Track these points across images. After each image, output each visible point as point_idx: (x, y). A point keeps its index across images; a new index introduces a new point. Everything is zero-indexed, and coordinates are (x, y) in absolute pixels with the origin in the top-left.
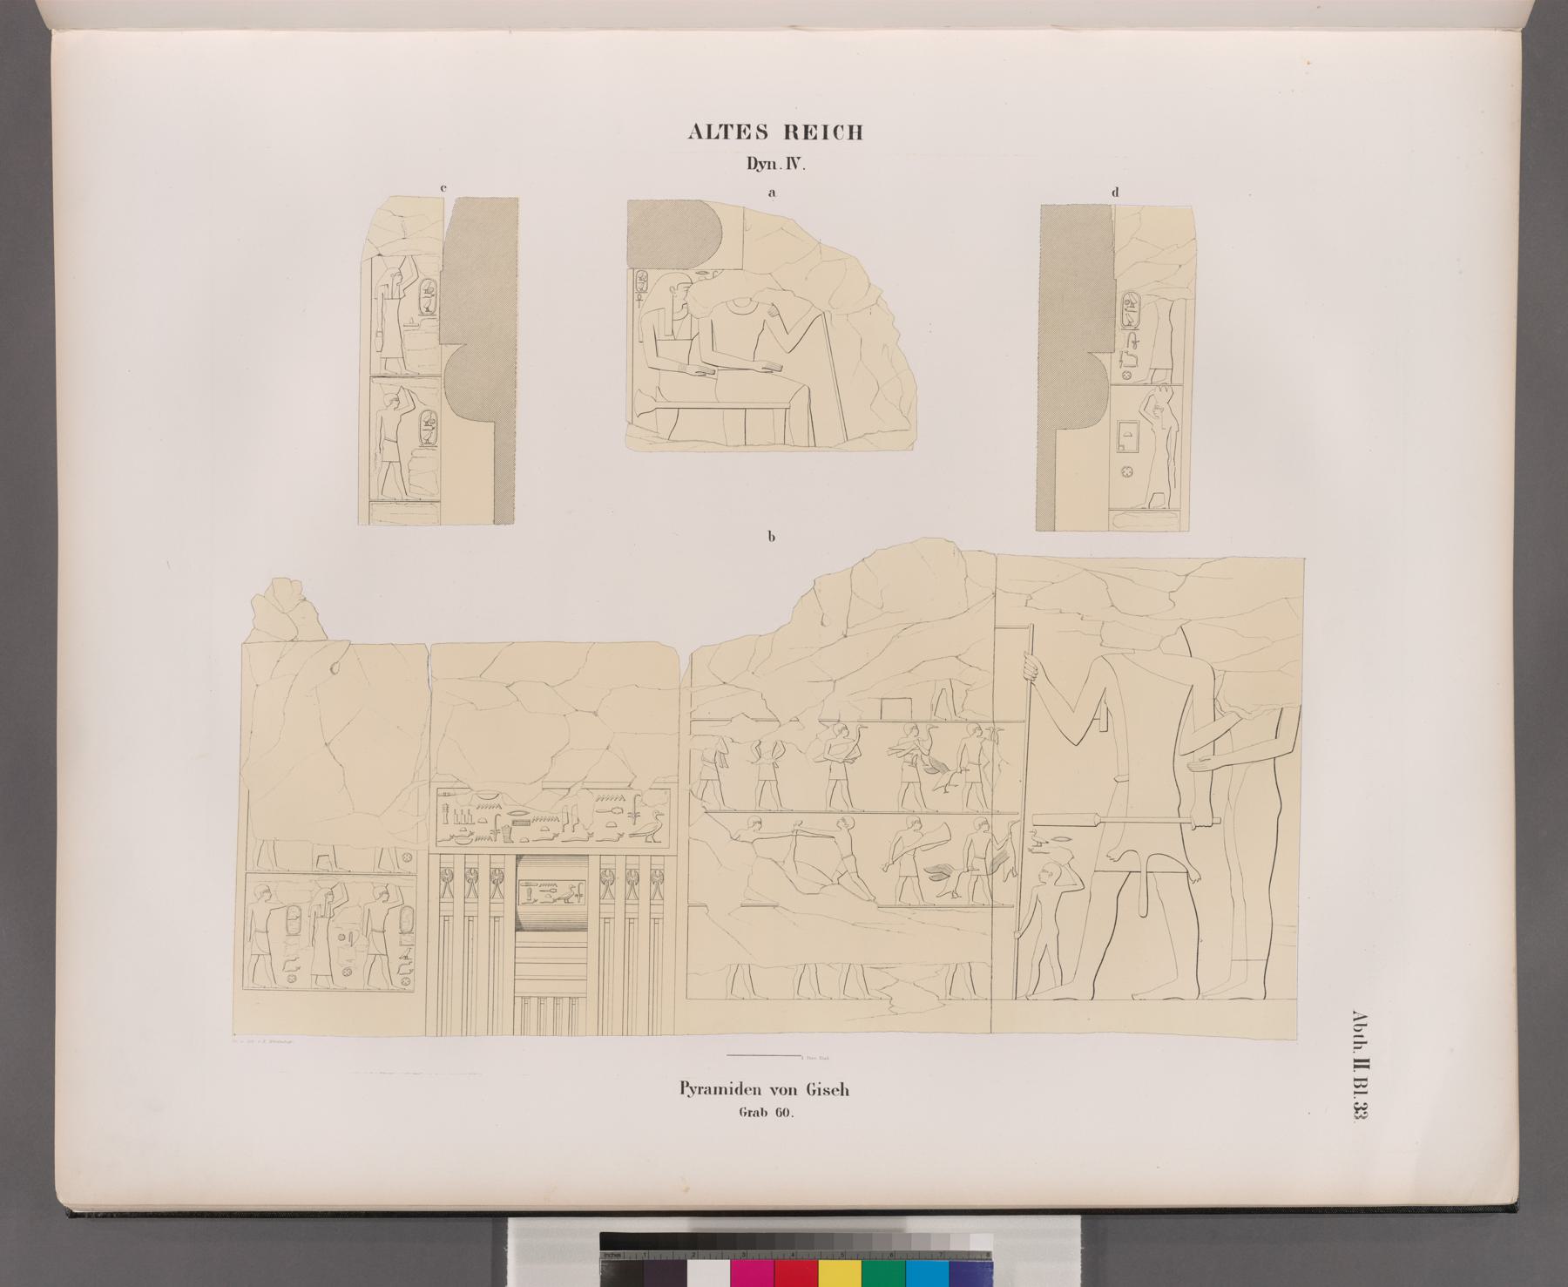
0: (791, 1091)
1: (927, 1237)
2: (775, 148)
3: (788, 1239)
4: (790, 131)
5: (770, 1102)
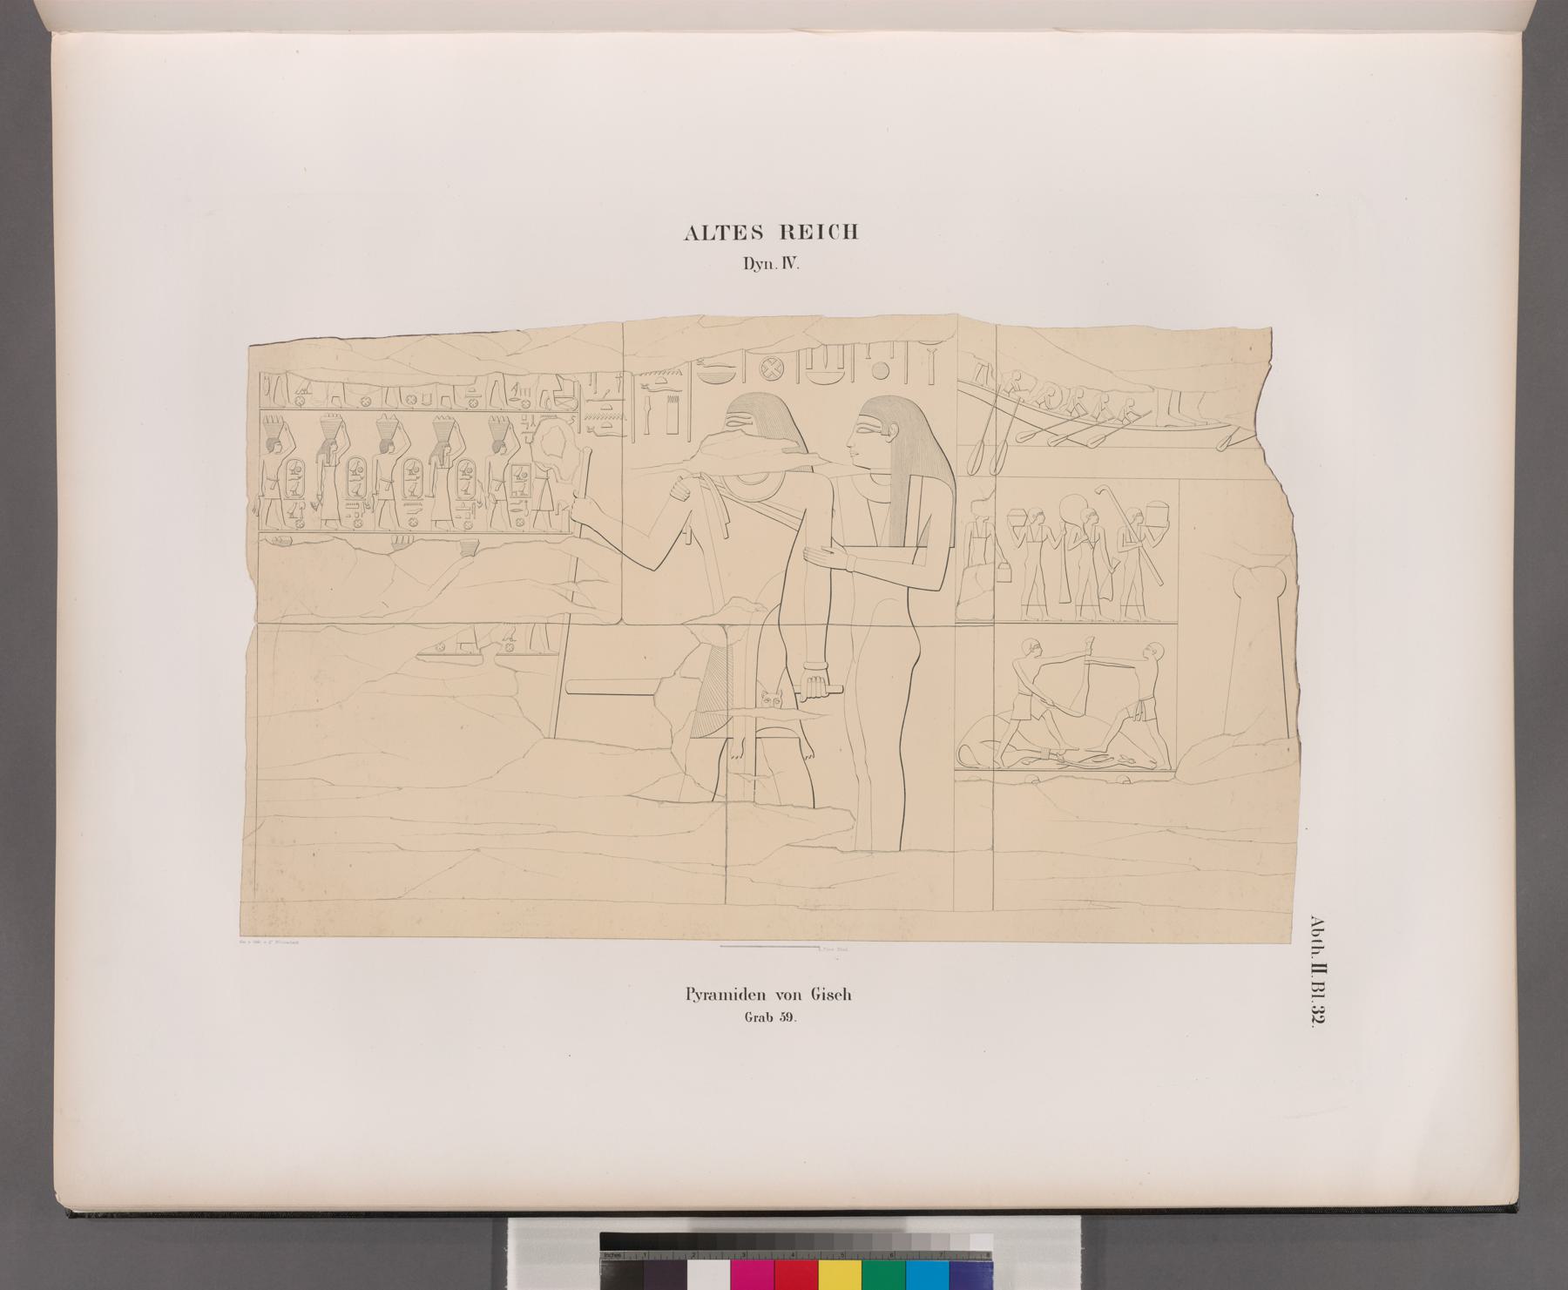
0: (796, 996)
2: (771, 248)
3: (789, 1239)
5: (776, 1007)
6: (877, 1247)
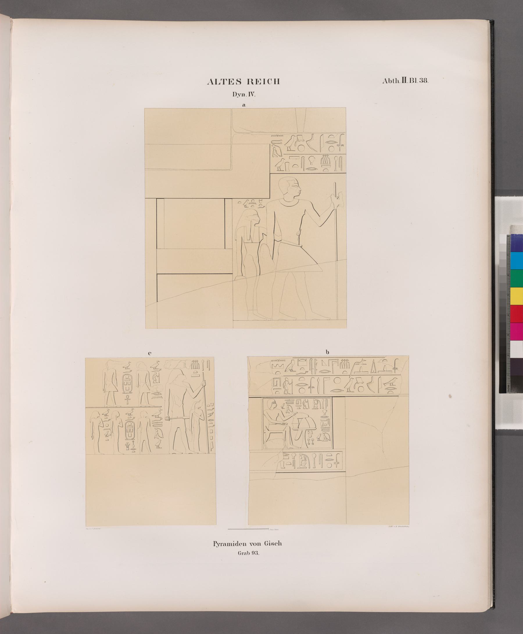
6: (505, 281)
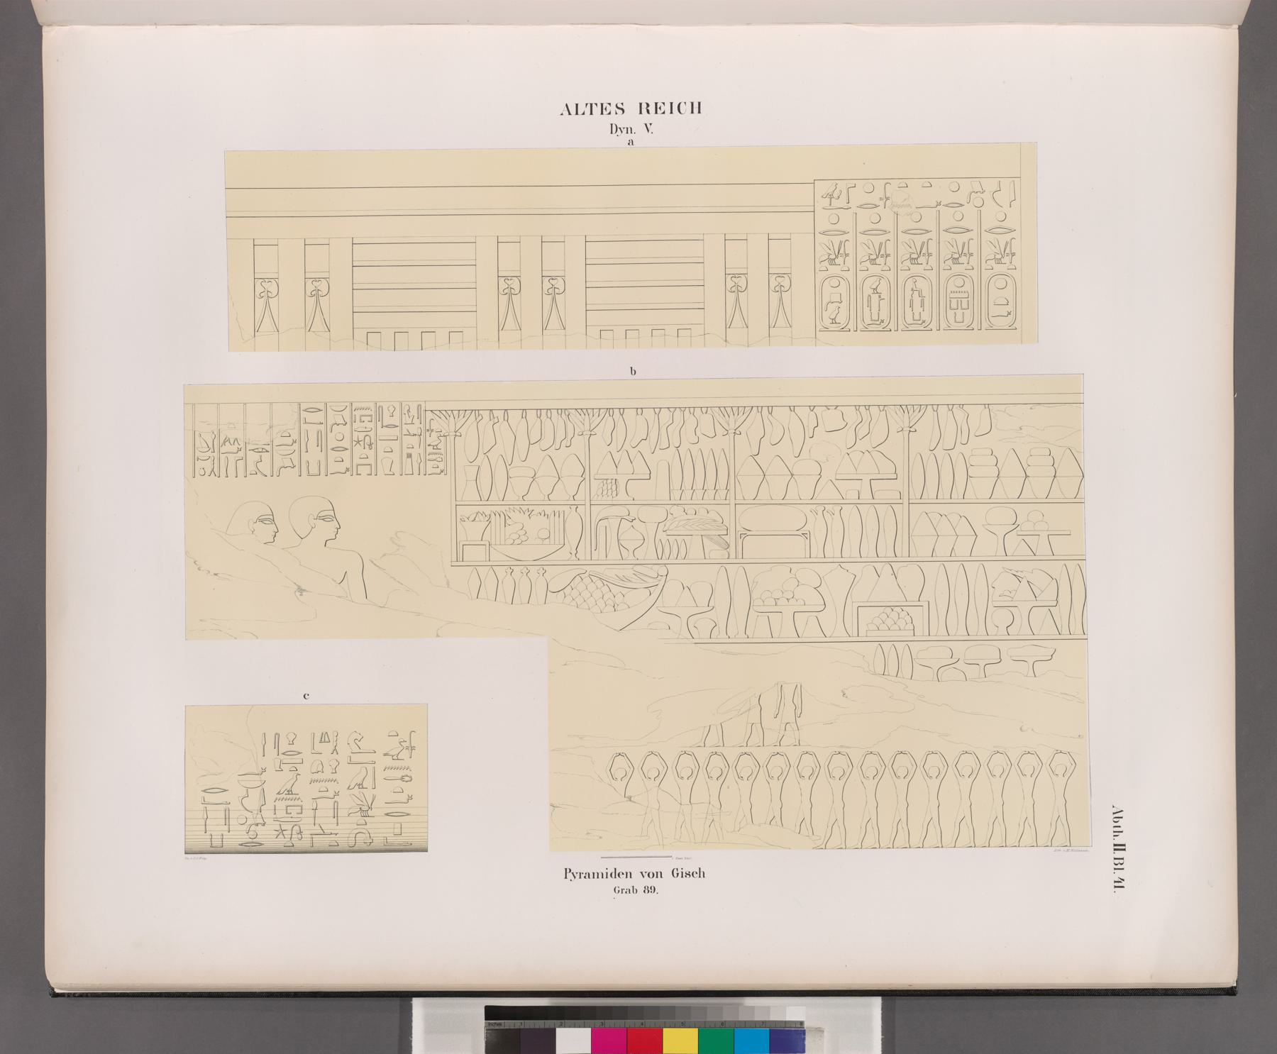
0: (658, 875)
1: (753, 1008)
3: (639, 1012)
4: (643, 108)
5: (640, 883)
6: (711, 1017)
